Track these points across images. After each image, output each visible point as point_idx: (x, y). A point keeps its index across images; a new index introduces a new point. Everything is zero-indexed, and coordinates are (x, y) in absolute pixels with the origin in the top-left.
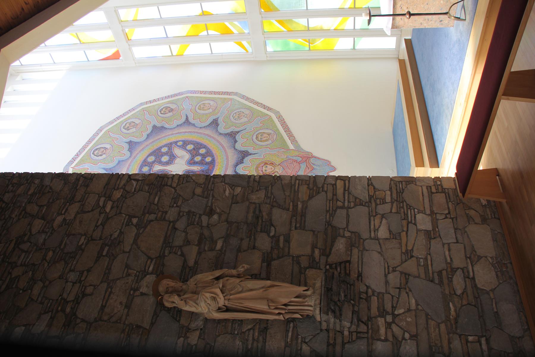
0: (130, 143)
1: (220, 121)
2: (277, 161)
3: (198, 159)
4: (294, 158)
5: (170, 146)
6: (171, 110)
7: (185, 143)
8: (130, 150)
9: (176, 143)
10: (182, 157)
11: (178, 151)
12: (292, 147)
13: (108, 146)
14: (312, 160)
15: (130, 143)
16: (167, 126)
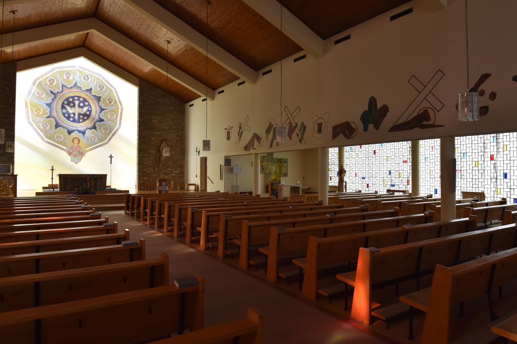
0: (91, 89)
1: (103, 122)
2: (80, 144)
3: (81, 117)
4: (81, 151)
5: (89, 105)
6: (110, 102)
7: (90, 111)
8: (87, 90)
9: (91, 107)
10: (82, 111)
11: (85, 109)
12: (87, 149)
13: (89, 81)
14: (80, 156)
15: (91, 89)
16: (100, 102)
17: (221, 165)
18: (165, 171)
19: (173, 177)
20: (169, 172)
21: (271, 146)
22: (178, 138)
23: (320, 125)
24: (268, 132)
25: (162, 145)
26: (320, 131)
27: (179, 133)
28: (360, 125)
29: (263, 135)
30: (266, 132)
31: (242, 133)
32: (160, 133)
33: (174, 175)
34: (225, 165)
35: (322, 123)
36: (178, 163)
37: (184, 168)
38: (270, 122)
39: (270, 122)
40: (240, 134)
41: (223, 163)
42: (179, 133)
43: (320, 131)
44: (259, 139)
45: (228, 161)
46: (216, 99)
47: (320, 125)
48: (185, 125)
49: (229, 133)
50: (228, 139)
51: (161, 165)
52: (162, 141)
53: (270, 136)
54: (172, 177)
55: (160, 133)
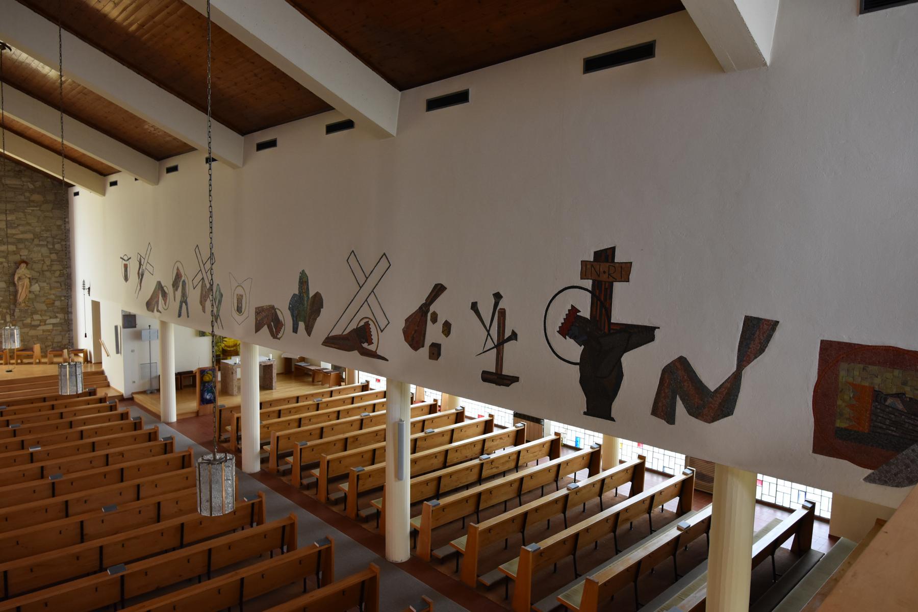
17: (116, 327)
18: (28, 321)
19: (48, 331)
20: (37, 323)
21: (180, 315)
22: (54, 256)
23: (240, 299)
24: (175, 285)
25: (18, 271)
26: (239, 310)
27: (57, 246)
28: (286, 317)
29: (169, 289)
30: (173, 285)
31: (142, 275)
32: (12, 248)
33: (50, 327)
34: (125, 326)
35: (242, 296)
36: (57, 303)
37: (71, 313)
38: (178, 269)
39: (178, 269)
40: (141, 276)
41: (120, 323)
42: (57, 246)
43: (239, 310)
44: (165, 295)
45: (129, 320)
46: (107, 195)
47: (240, 299)
48: (69, 230)
49: (126, 266)
50: (126, 279)
51: (17, 310)
52: (18, 264)
53: (179, 293)
54: (44, 331)
55: (12, 248)
